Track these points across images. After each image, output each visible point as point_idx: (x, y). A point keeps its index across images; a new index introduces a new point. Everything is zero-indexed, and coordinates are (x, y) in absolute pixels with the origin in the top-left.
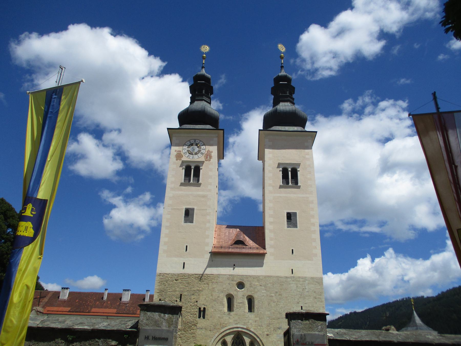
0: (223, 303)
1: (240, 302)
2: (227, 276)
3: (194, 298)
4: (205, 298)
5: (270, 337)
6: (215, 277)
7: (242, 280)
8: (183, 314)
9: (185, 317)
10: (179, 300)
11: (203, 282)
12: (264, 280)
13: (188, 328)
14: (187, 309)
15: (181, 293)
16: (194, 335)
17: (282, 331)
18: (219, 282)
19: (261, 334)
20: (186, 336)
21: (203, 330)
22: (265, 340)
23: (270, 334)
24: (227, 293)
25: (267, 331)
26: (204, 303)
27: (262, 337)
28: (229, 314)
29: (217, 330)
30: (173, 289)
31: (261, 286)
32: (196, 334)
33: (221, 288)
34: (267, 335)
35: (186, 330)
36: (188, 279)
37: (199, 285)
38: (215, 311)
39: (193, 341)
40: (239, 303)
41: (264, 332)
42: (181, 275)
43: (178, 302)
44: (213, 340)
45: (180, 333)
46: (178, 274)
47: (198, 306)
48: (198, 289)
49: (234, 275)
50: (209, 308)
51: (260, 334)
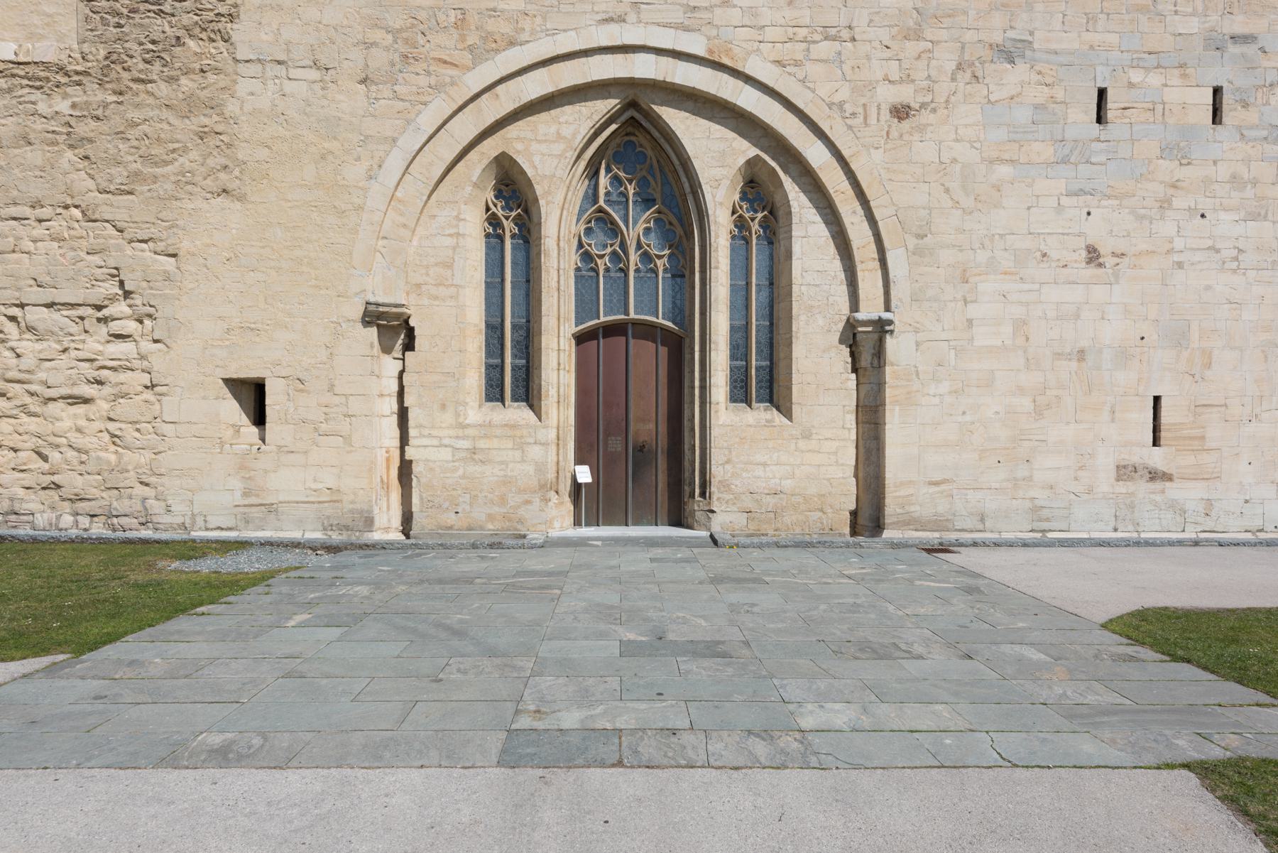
5: (921, 129)
13: (146, 62)
16: (210, 121)
17: (1035, 77)
19: (841, 105)
20: (132, 133)
21: (295, 73)
22: (877, 156)
23: (923, 105)
25: (901, 81)
27: (850, 127)
29: (428, 73)
32: (232, 108)
34: (901, 112)
35: (125, 75)
39: (211, 172)
41: (871, 86)
44: (395, 162)
45: (68, 103)
51: (830, 106)
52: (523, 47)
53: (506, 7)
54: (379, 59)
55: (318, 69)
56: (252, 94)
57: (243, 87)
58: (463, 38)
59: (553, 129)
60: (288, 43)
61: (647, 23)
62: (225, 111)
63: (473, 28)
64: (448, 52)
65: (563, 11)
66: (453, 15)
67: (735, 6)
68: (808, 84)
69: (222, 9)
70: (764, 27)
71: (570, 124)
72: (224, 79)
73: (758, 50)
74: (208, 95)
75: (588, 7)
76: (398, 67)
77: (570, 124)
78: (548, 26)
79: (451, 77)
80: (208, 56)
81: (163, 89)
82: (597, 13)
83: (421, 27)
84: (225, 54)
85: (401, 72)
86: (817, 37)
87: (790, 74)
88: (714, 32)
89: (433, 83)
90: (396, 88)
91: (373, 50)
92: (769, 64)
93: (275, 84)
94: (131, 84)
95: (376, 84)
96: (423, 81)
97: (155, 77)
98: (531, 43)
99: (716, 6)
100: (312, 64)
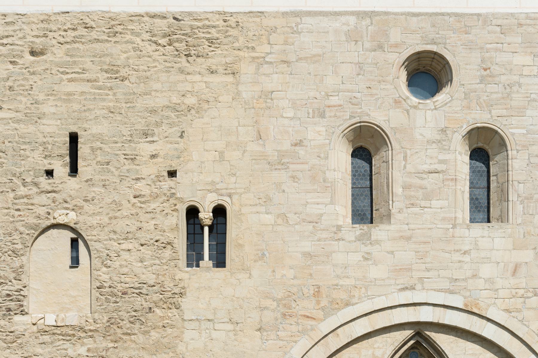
0: (329, 175)
1: (426, 167)
2: (343, 19)
3: (153, 156)
4: (221, 153)
6: (274, 29)
7: (435, 43)
8: (98, 245)
9: (109, 263)
10: (64, 166)
11: (200, 60)
14: (118, 214)
15: (74, 129)
18: (299, 59)
21: (217, 326)
24: (351, 117)
26: (217, 180)
28: (364, 238)
29: (297, 324)
30: (22, 107)
33: (312, 94)
35: (119, 331)
36: (108, 45)
37: (182, 77)
38: (280, 221)
40: (419, 174)
42: (61, 18)
43: (60, 178)
46: (42, 18)
47: (181, 200)
48: (175, 99)
49: (386, 13)
50: (244, 210)
52: (354, 306)
53: (344, 283)
54: (268, 317)
55: (232, 323)
56: (193, 339)
57: (188, 335)
58: (318, 302)
59: (370, 352)
60: (215, 309)
61: (428, 290)
62: (177, 350)
63: (324, 296)
64: (309, 311)
65: (378, 284)
66: (313, 289)
67: (480, 278)
68: (525, 323)
69: (177, 290)
70: (498, 289)
71: (380, 348)
72: (176, 331)
73: (495, 303)
74: (167, 341)
75: (393, 282)
76: (279, 321)
77: (380, 348)
78: (369, 294)
79: (311, 326)
80: (167, 317)
81: (141, 338)
82: (398, 285)
83: (294, 297)
84: (177, 316)
85: (281, 323)
86: (530, 294)
87: (514, 317)
88: (468, 294)
89: (300, 329)
90: (279, 333)
91: (266, 312)
92: (501, 312)
93: (206, 333)
94: (122, 336)
95: (267, 331)
96: (294, 328)
97: (136, 332)
98: (359, 304)
99: (469, 278)
100: (229, 320)
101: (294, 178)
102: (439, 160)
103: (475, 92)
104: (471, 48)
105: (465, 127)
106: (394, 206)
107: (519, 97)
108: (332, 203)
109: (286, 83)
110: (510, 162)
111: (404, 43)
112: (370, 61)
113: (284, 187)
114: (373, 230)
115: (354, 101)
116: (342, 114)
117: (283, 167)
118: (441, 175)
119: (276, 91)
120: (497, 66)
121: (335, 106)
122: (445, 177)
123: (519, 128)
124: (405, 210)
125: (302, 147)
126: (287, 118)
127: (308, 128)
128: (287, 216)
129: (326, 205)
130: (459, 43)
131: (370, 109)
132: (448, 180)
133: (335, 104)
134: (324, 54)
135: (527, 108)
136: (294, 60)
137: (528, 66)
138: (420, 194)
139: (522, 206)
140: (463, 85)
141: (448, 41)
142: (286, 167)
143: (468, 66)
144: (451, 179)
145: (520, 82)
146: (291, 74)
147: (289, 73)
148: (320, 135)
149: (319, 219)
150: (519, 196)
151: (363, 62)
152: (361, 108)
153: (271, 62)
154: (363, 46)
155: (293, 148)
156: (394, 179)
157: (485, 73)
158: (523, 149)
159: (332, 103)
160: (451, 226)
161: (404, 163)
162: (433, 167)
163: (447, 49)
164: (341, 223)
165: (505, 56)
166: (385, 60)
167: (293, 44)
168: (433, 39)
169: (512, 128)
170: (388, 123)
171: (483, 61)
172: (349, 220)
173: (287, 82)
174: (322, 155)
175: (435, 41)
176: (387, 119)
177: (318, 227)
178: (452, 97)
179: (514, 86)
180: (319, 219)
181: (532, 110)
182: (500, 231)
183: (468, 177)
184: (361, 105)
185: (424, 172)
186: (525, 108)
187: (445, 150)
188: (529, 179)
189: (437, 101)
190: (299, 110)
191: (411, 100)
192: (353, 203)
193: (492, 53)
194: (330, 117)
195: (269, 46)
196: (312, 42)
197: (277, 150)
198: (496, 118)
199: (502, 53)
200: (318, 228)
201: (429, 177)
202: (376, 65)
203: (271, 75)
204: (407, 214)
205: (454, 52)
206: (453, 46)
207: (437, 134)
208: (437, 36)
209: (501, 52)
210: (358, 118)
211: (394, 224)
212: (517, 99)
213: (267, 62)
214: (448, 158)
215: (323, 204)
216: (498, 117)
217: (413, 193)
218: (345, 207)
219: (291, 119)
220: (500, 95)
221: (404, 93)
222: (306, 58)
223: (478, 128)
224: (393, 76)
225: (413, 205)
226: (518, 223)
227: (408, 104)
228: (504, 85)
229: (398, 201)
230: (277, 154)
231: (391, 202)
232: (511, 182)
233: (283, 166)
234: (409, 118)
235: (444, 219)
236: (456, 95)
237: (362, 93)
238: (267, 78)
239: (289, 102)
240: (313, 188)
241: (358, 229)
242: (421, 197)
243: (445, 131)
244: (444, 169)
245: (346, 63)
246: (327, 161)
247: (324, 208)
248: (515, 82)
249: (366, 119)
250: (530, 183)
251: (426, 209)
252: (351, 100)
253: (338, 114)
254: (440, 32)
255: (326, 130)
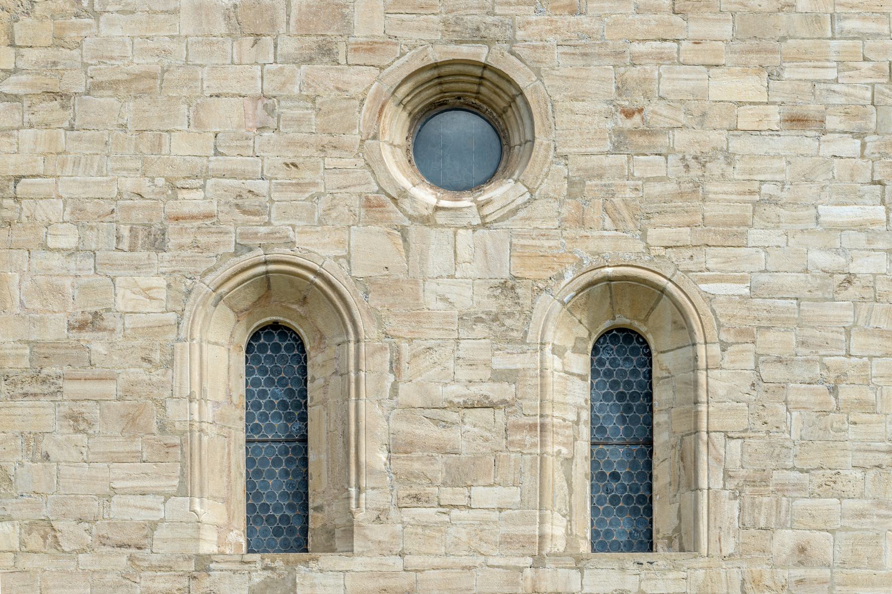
0: (175, 412)
1: (456, 391)
7: (483, 40)
12: (848, 25)
18: (96, 87)
24: (241, 248)
31: (797, 121)
33: (129, 183)
38: (35, 541)
101: (76, 420)
102: (494, 371)
103: (600, 177)
104: (585, 55)
105: (569, 276)
106: (362, 501)
107: (725, 193)
108: (184, 491)
109: (58, 154)
110: (702, 376)
111: (394, 40)
112: (296, 90)
113: (47, 445)
114: (301, 568)
115: (249, 202)
116: (214, 239)
117: (45, 388)
118: (500, 415)
119: (28, 177)
120: (662, 102)
121: (193, 218)
122: (512, 419)
123: (727, 281)
124: (394, 514)
125: (100, 334)
126: (59, 250)
127: (118, 280)
128: (56, 527)
129: (167, 497)
130: (552, 39)
131: (294, 227)
132: (519, 427)
133: (195, 211)
134: (164, 71)
135: (750, 223)
136: (82, 89)
137: (751, 103)
138: (438, 468)
139: (736, 504)
140: (566, 157)
141: (520, 34)
142: (53, 388)
143: (578, 106)
144: (530, 426)
145: (731, 150)
146: (72, 128)
147: (66, 124)
148: (151, 298)
149: (146, 537)
150: (727, 475)
151: (274, 93)
152: (268, 223)
153: (16, 96)
154: (276, 47)
155: (74, 334)
156: (362, 425)
157: (628, 124)
158: (740, 340)
159: (186, 209)
160: (529, 561)
161: (391, 378)
162: (476, 391)
163: (518, 57)
164: (208, 547)
165: (686, 76)
166: (338, 89)
167: (79, 45)
168: (478, 29)
169: (706, 280)
170: (345, 265)
171: (622, 89)
172: (238, 537)
173: (60, 150)
174: (157, 357)
175: (483, 33)
176: (345, 253)
177: (144, 560)
178: (531, 191)
179: (713, 159)
180: (146, 537)
181: (766, 228)
182: (671, 575)
183: (586, 415)
184: (269, 215)
185: (451, 405)
186: (744, 224)
187: (510, 341)
188: (758, 425)
189: (489, 202)
190: (92, 228)
191: (413, 199)
192: (250, 486)
193: (647, 67)
194: (181, 247)
195: (12, 51)
196: (132, 38)
197: (28, 342)
198: (662, 252)
199: (678, 68)
200: (141, 564)
201: (466, 420)
202: (314, 101)
203: (15, 132)
204: (399, 527)
205: (538, 65)
206: (535, 48)
207: (489, 296)
208: (489, 19)
209: (673, 64)
210: (261, 251)
211: (361, 554)
212: (720, 196)
213: (6, 95)
214: (519, 366)
215: (158, 493)
216: (666, 247)
217: (417, 466)
218: (226, 501)
219: (70, 253)
220: (671, 187)
221: (392, 180)
222: (113, 84)
223: (609, 279)
224: (360, 132)
225: (419, 500)
226: (725, 553)
227: (403, 211)
228: (683, 158)
229: (373, 488)
230: (28, 351)
231: (353, 491)
232: (704, 436)
233: (45, 387)
234: (407, 251)
235: (507, 541)
236: (544, 186)
237: (271, 179)
238: (5, 139)
239: (64, 206)
240: (128, 449)
241: (259, 566)
242: (440, 477)
243: (513, 288)
244: (508, 398)
245: (226, 95)
246: (170, 371)
247: (162, 507)
248: (714, 149)
249: (280, 252)
250: (761, 438)
251: (455, 513)
252: (239, 201)
253: (203, 239)
254: (497, 11)
255: (169, 286)
